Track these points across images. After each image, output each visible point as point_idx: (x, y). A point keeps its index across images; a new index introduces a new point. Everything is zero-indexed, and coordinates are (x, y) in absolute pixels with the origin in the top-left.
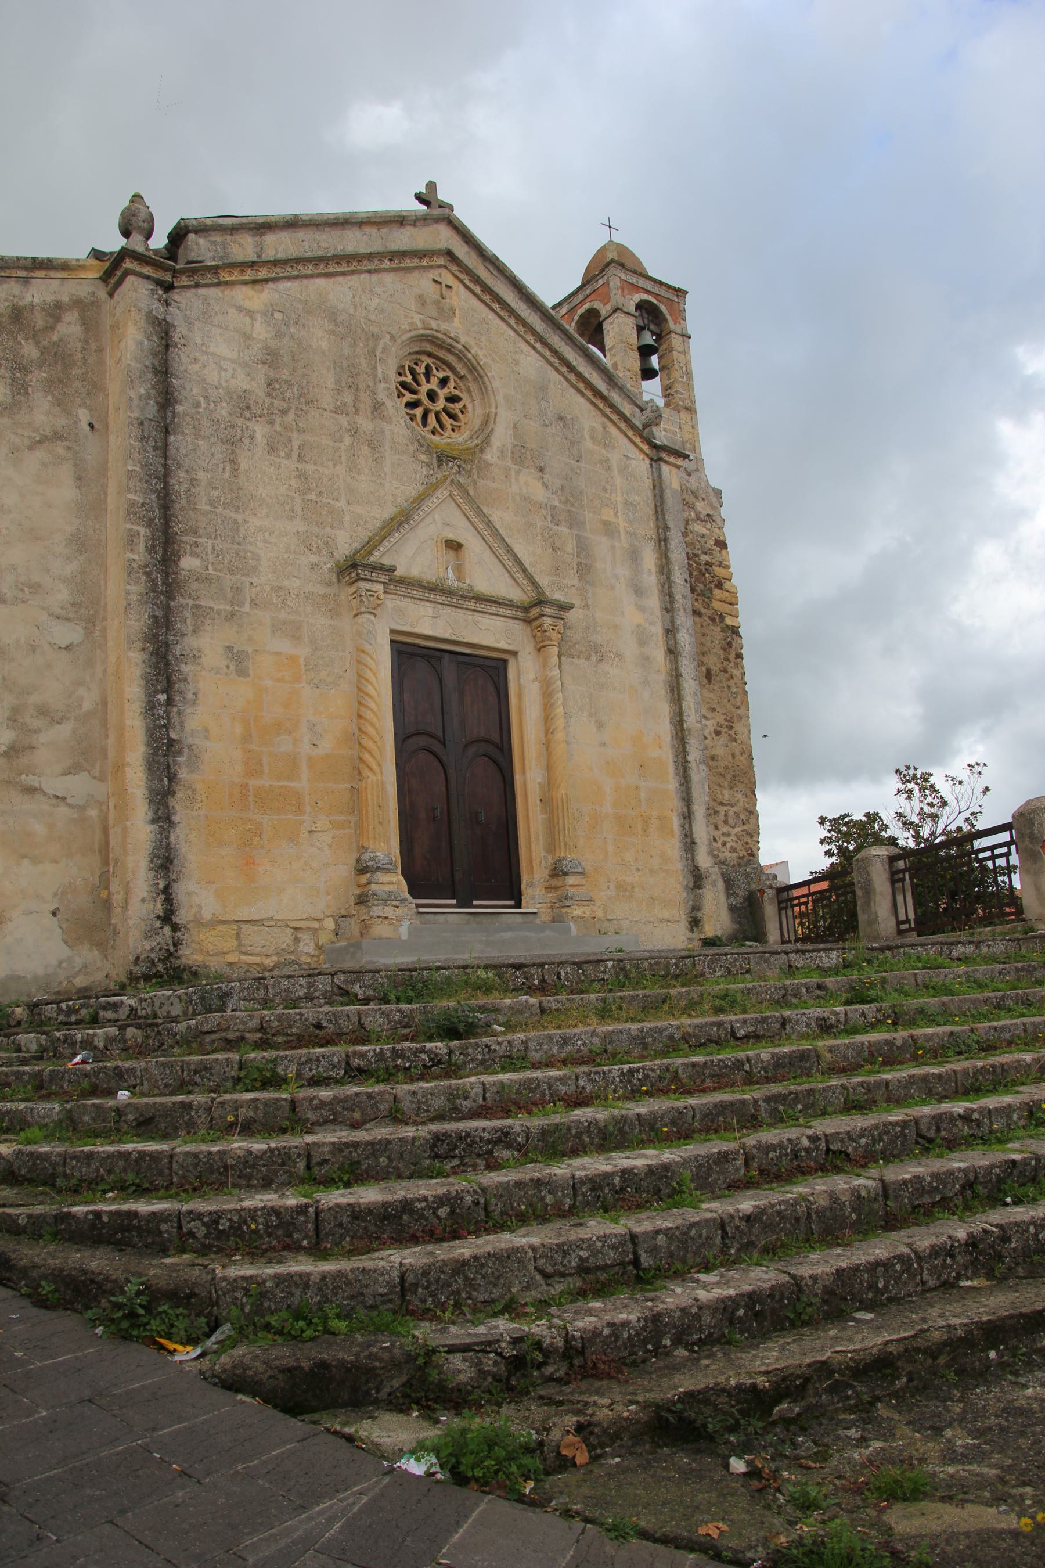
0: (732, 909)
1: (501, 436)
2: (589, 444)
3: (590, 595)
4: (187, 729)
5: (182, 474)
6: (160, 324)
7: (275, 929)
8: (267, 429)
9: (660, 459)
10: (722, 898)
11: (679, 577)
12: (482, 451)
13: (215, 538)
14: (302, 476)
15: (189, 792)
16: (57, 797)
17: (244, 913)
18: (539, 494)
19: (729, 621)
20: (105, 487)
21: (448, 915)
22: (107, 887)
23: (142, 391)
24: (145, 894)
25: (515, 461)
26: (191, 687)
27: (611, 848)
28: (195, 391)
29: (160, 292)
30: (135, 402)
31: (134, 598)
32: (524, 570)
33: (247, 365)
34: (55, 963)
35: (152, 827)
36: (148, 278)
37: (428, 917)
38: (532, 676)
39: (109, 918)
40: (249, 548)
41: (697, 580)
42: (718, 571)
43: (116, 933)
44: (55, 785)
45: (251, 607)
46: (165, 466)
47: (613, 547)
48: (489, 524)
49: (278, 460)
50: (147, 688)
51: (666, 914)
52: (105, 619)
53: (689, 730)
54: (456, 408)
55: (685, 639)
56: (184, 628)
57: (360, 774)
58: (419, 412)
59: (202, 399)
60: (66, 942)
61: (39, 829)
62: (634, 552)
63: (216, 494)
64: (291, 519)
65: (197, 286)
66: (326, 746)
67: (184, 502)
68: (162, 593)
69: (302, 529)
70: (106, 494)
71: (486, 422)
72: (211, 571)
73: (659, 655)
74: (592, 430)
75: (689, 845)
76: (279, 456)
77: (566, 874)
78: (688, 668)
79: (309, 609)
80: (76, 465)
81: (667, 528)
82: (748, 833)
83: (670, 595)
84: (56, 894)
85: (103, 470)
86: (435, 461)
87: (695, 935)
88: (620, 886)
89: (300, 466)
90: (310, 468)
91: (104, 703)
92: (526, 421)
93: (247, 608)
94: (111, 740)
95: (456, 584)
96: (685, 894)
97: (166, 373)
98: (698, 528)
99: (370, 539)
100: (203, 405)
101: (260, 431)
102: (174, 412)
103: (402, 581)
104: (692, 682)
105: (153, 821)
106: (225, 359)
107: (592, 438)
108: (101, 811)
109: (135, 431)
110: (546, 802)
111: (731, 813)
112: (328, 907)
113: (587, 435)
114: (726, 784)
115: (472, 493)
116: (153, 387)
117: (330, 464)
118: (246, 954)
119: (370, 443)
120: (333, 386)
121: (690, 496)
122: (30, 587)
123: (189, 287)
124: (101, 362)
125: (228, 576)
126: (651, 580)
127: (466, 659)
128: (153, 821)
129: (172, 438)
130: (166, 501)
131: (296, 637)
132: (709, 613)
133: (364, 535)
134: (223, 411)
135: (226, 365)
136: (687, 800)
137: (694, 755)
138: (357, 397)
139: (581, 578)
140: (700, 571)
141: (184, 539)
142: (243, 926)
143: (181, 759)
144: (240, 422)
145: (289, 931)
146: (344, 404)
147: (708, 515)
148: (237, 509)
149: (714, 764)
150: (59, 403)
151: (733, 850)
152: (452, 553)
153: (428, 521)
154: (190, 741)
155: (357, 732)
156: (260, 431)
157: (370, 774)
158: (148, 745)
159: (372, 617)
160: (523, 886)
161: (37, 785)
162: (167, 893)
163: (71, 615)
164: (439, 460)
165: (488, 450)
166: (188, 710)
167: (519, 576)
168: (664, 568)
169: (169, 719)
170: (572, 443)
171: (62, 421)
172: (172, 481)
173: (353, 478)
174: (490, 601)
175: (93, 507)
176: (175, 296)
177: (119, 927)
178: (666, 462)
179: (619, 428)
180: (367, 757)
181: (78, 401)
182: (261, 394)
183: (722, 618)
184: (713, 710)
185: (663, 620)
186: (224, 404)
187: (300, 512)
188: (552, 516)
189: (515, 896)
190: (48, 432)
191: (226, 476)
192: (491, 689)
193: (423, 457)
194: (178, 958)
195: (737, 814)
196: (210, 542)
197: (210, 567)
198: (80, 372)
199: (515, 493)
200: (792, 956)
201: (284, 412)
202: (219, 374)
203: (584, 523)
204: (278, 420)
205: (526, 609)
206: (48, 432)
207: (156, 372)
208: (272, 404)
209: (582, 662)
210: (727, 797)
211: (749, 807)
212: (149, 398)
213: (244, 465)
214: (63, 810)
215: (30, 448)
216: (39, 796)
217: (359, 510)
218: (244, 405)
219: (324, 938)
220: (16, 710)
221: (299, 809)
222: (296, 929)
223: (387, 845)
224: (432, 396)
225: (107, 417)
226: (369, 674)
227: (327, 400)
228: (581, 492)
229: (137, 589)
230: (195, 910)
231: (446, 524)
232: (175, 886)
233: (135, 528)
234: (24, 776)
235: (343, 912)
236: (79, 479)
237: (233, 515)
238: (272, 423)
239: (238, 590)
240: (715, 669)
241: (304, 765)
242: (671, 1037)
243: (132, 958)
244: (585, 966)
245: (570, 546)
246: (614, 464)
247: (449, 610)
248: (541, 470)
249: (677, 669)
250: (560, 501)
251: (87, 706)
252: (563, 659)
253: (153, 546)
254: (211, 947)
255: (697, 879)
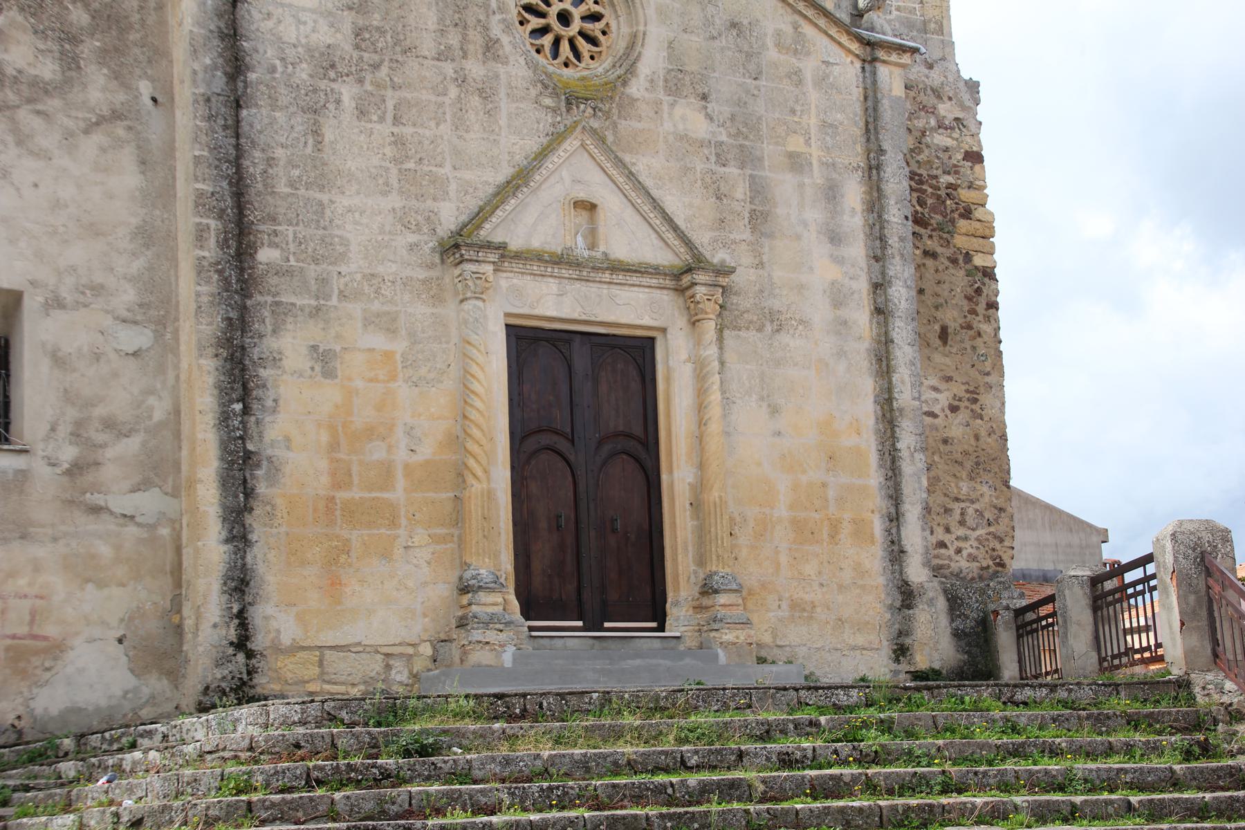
0: (957, 634)
1: (652, 60)
2: (772, 54)
3: (766, 249)
4: (267, 439)
5: (257, 154)
7: (363, 655)
8: (356, 89)
9: (875, 60)
10: (944, 620)
11: (896, 215)
12: (625, 83)
13: (297, 224)
14: (399, 142)
15: (268, 508)
16: (125, 516)
17: (328, 638)
18: (699, 127)
19: (978, 261)
20: (172, 169)
21: (570, 637)
22: (179, 612)
23: (208, 61)
24: (217, 620)
25: (669, 91)
26: (271, 394)
27: (783, 559)
28: (269, 53)
30: (200, 75)
31: (205, 299)
32: (675, 228)
33: (330, 13)
34: (119, 693)
35: (225, 548)
37: (542, 641)
38: (684, 356)
39: (181, 645)
40: (337, 232)
41: (934, 209)
42: (965, 194)
43: (187, 661)
44: (121, 502)
45: (339, 300)
46: (237, 147)
47: (801, 186)
48: (631, 176)
49: (369, 126)
50: (220, 397)
51: (860, 640)
52: (177, 319)
53: (901, 410)
54: (594, 28)
55: (901, 295)
56: (262, 329)
57: (464, 481)
58: (547, 40)
59: (278, 62)
60: (132, 671)
61: (105, 550)
62: (831, 188)
63: (296, 173)
64: (385, 194)
66: (426, 451)
67: (260, 186)
68: (236, 292)
69: (398, 205)
70: (174, 178)
71: (631, 46)
72: (293, 262)
73: (861, 317)
74: (778, 34)
75: (896, 553)
76: (370, 121)
77: (716, 592)
78: (902, 332)
79: (407, 297)
80: (139, 147)
81: (881, 151)
82: (996, 537)
83: (882, 238)
84: (122, 620)
85: (170, 150)
86: (563, 104)
87: (900, 667)
88: (795, 606)
89: (396, 130)
90: (408, 130)
91: (177, 412)
92: (686, 36)
93: (334, 301)
94: (184, 453)
95: (586, 253)
96: (888, 616)
97: (235, 35)
98: (941, 139)
99: (481, 209)
100: (280, 69)
101: (348, 92)
102: (245, 82)
103: (518, 256)
104: (908, 349)
105: (227, 541)
106: (304, 9)
107: (777, 45)
108: (174, 529)
109: (202, 110)
110: (696, 505)
111: (970, 511)
112: (426, 630)
113: (770, 42)
114: (964, 475)
115: (610, 138)
116: (221, 55)
117: (433, 124)
118: (329, 682)
119: (481, 91)
120: (435, 27)
121: (922, 98)
122: (92, 289)
124: (162, 23)
125: (313, 266)
126: (854, 218)
127: (602, 341)
128: (227, 541)
129: (244, 113)
130: (239, 187)
131: (392, 331)
132: (948, 252)
133: (473, 204)
134: (303, 74)
135: (305, 16)
136: (895, 497)
137: (907, 440)
138: (464, 36)
139: (754, 229)
140: (939, 197)
141: (262, 227)
142: (327, 652)
143: (259, 473)
144: (323, 84)
145: (379, 657)
146: (449, 48)
147: (957, 119)
148: (322, 188)
149: (948, 448)
150: (116, 76)
151: (972, 558)
152: (585, 214)
153: (552, 180)
154: (269, 452)
155: (462, 435)
156: (348, 92)
157: (474, 482)
158: (222, 459)
159: (480, 303)
160: (668, 606)
161: (103, 504)
162: (242, 619)
163: (139, 318)
164: (569, 103)
165: (634, 81)
166: (267, 419)
167: (670, 236)
168: (875, 204)
169: (245, 429)
170: (749, 56)
171: (121, 97)
172: (246, 163)
173: (460, 137)
174: (629, 270)
175: (160, 194)
177: (190, 655)
178: (884, 62)
179: (816, 25)
180: (471, 462)
181: (138, 72)
182: (348, 47)
183: (968, 257)
184: (949, 379)
185: (869, 272)
186: (304, 65)
187: (396, 185)
188: (718, 155)
189: (659, 616)
190: (106, 112)
191: (309, 150)
192: (633, 372)
193: (548, 101)
194: (253, 687)
195: (980, 513)
196: (291, 229)
197: (291, 258)
198: (138, 36)
199: (668, 128)
200: (802, 693)
201: (376, 67)
202: (298, 29)
203: (761, 159)
204: (369, 77)
205: (677, 277)
206: (106, 112)
207: (223, 36)
208: (361, 58)
209: (752, 335)
210: (965, 490)
211: (1000, 502)
212: (216, 68)
213: (329, 135)
214: (132, 530)
215: (86, 132)
216: (105, 516)
217: (468, 175)
218: (327, 64)
219: (418, 666)
220: (79, 424)
221: (394, 523)
222: (387, 655)
223: (497, 557)
224: (564, 18)
225: (172, 87)
226: (475, 369)
227: (428, 46)
228: (760, 118)
229: (209, 288)
230: (273, 635)
231: (576, 181)
232: (251, 609)
233: (205, 221)
234: (88, 495)
235: (443, 636)
236: (143, 163)
237: (318, 196)
238: (361, 81)
239: (323, 281)
240: (952, 326)
241: (399, 474)
242: (615, 763)
243: (200, 688)
244: (568, 697)
245: (741, 191)
246: (808, 76)
247: (578, 285)
248: (704, 97)
249: (886, 333)
250: (729, 135)
251: (158, 415)
252: (726, 333)
253: (226, 240)
254: (289, 675)
255: (907, 596)
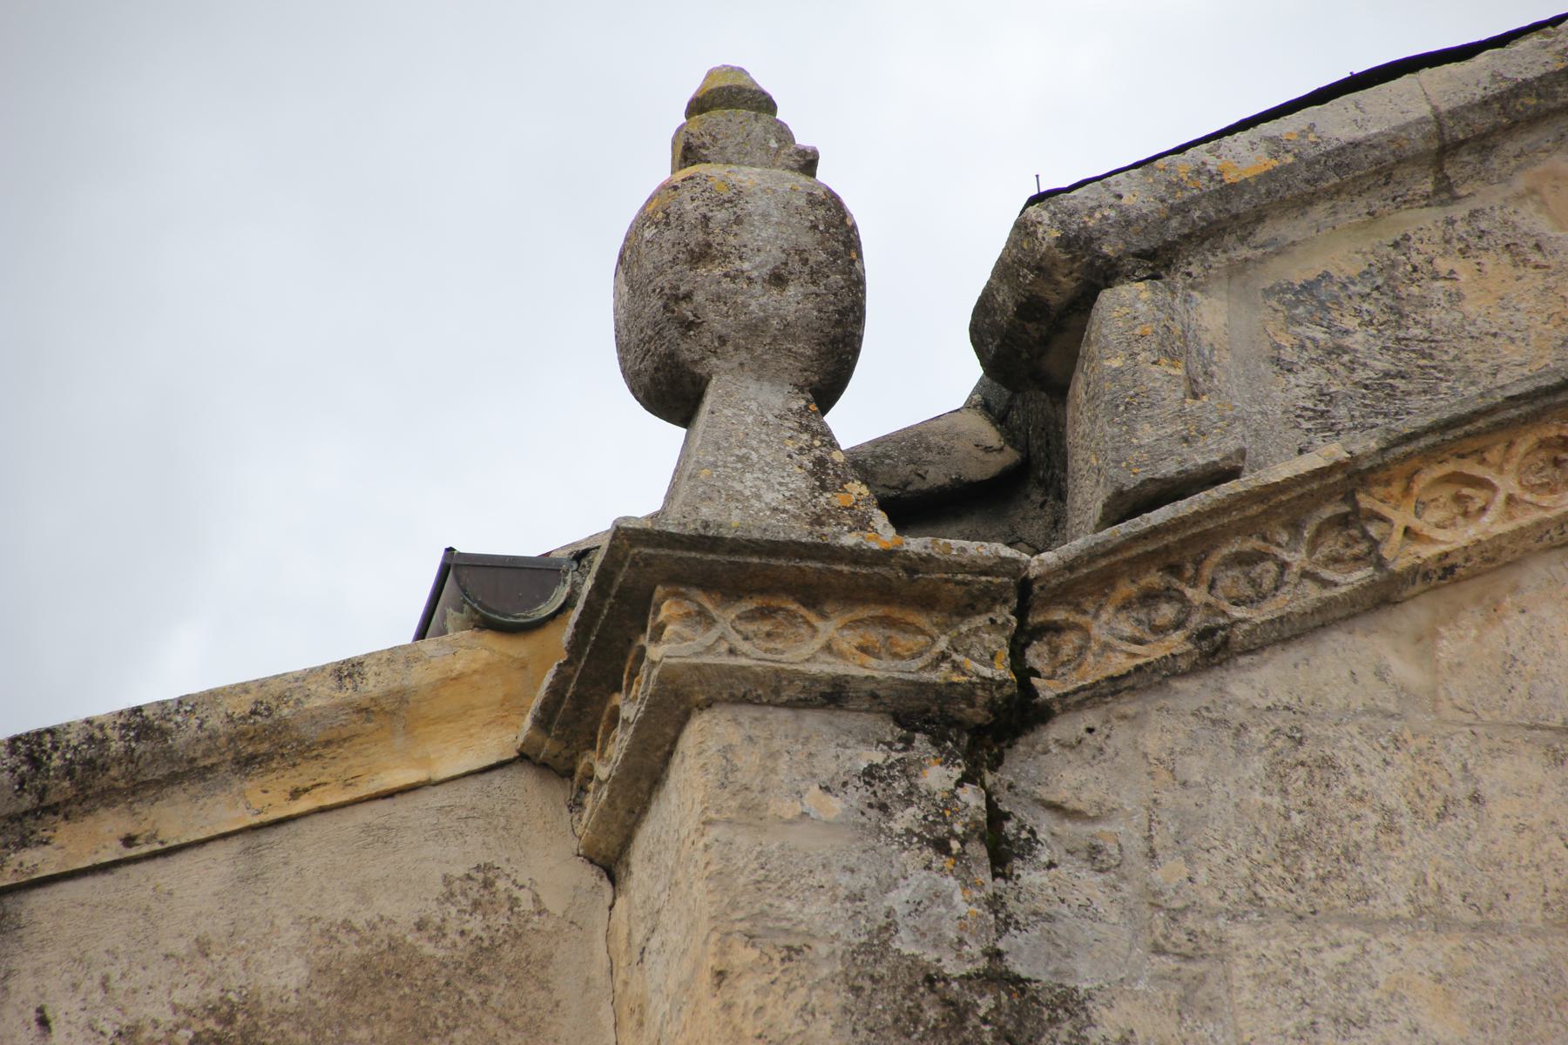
6: (958, 1013)
29: (937, 777)
36: (833, 696)
65: (1216, 650)
123: (1149, 679)
176: (1056, 770)
